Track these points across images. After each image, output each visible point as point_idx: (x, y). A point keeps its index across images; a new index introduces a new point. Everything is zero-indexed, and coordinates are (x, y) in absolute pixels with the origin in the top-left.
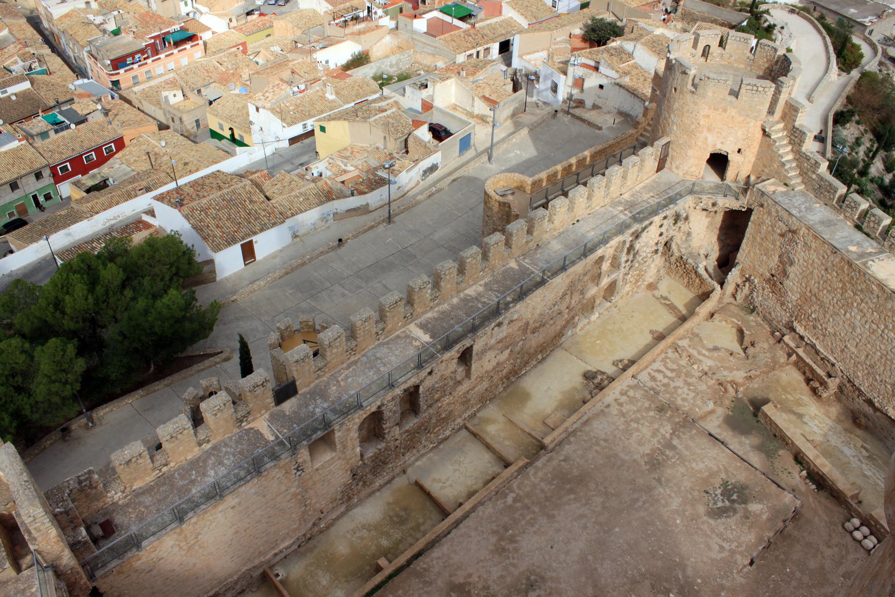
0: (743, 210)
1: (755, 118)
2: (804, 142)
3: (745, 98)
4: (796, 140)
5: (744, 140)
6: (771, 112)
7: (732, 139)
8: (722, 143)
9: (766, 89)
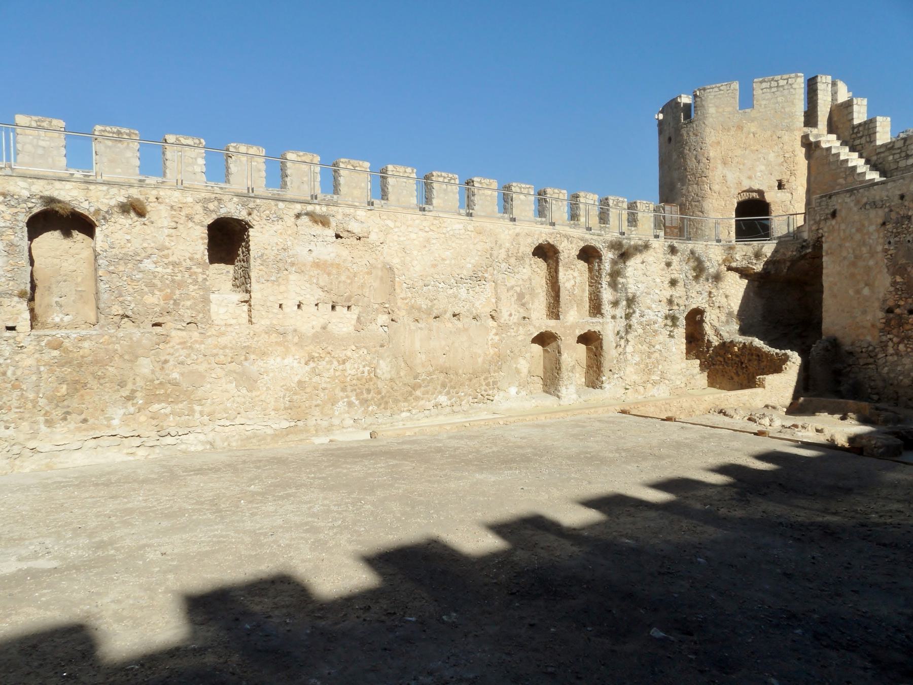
0: (809, 250)
1: (789, 129)
2: (875, 133)
3: (764, 102)
4: (863, 141)
5: (781, 164)
6: (810, 119)
7: (763, 168)
8: (750, 178)
9: (790, 81)
